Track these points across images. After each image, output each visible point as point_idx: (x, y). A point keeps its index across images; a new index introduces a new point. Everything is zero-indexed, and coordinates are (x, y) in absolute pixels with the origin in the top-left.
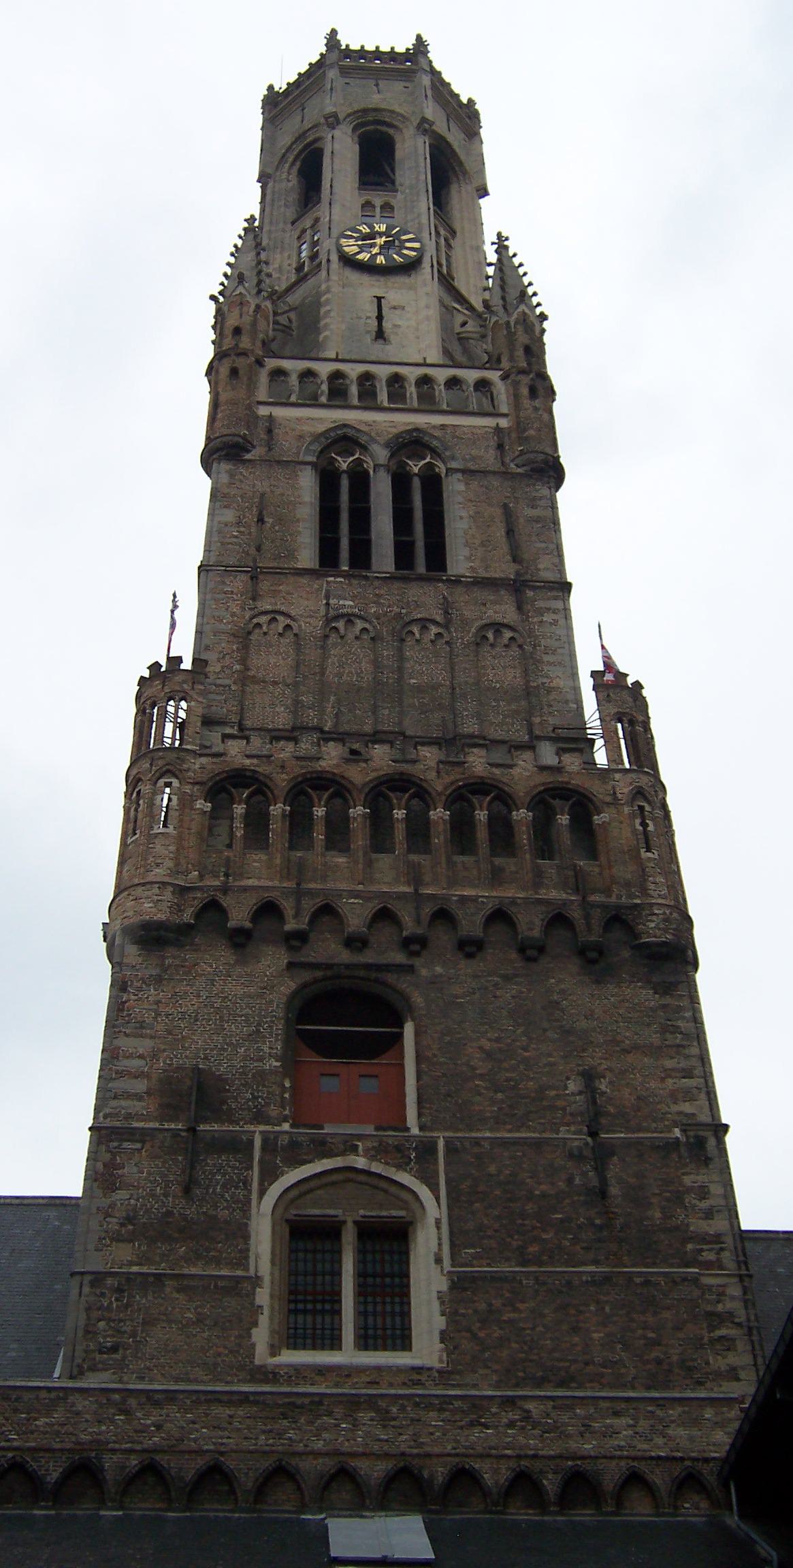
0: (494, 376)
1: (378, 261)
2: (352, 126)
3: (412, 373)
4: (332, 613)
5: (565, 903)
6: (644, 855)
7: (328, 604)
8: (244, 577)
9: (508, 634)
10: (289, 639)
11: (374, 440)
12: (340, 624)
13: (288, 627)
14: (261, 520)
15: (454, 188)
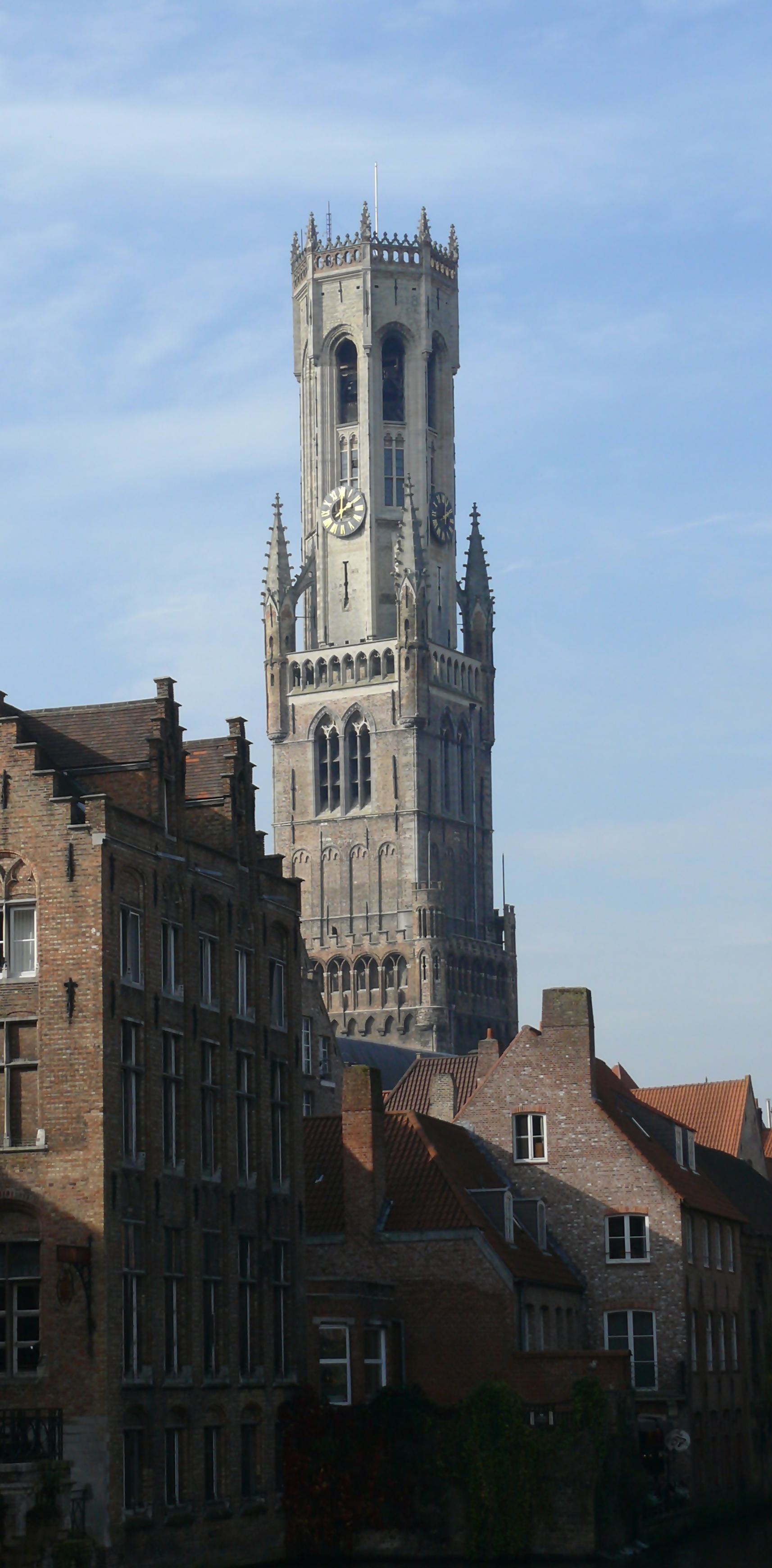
0: (392, 644)
1: (342, 533)
2: (329, 348)
3: (354, 652)
4: (324, 847)
5: (392, 1011)
6: (423, 982)
7: (322, 842)
8: (289, 829)
9: (392, 847)
10: (308, 865)
11: (336, 717)
12: (326, 853)
13: (307, 857)
14: (294, 789)
15: (406, 357)
